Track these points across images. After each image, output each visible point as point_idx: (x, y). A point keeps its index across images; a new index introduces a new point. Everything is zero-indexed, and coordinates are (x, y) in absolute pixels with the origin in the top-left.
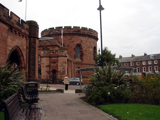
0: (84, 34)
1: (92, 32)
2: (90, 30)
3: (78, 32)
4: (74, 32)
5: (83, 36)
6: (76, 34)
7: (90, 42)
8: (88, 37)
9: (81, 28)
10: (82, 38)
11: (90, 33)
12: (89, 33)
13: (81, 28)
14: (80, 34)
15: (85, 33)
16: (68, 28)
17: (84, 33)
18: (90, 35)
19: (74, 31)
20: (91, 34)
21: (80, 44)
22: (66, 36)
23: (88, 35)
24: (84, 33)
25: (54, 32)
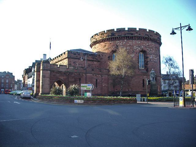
0: (120, 37)
1: (132, 32)
2: (130, 30)
3: (111, 36)
4: (107, 37)
5: (119, 40)
6: (109, 38)
7: (130, 46)
8: (126, 39)
9: (115, 30)
10: (118, 43)
11: (130, 34)
12: (128, 34)
13: (115, 30)
14: (113, 38)
15: (121, 35)
16: (102, 34)
17: (119, 35)
18: (129, 37)
19: (107, 36)
20: (132, 34)
21: (116, 50)
22: (101, 43)
23: (126, 37)
24: (119, 35)
25: (92, 42)
